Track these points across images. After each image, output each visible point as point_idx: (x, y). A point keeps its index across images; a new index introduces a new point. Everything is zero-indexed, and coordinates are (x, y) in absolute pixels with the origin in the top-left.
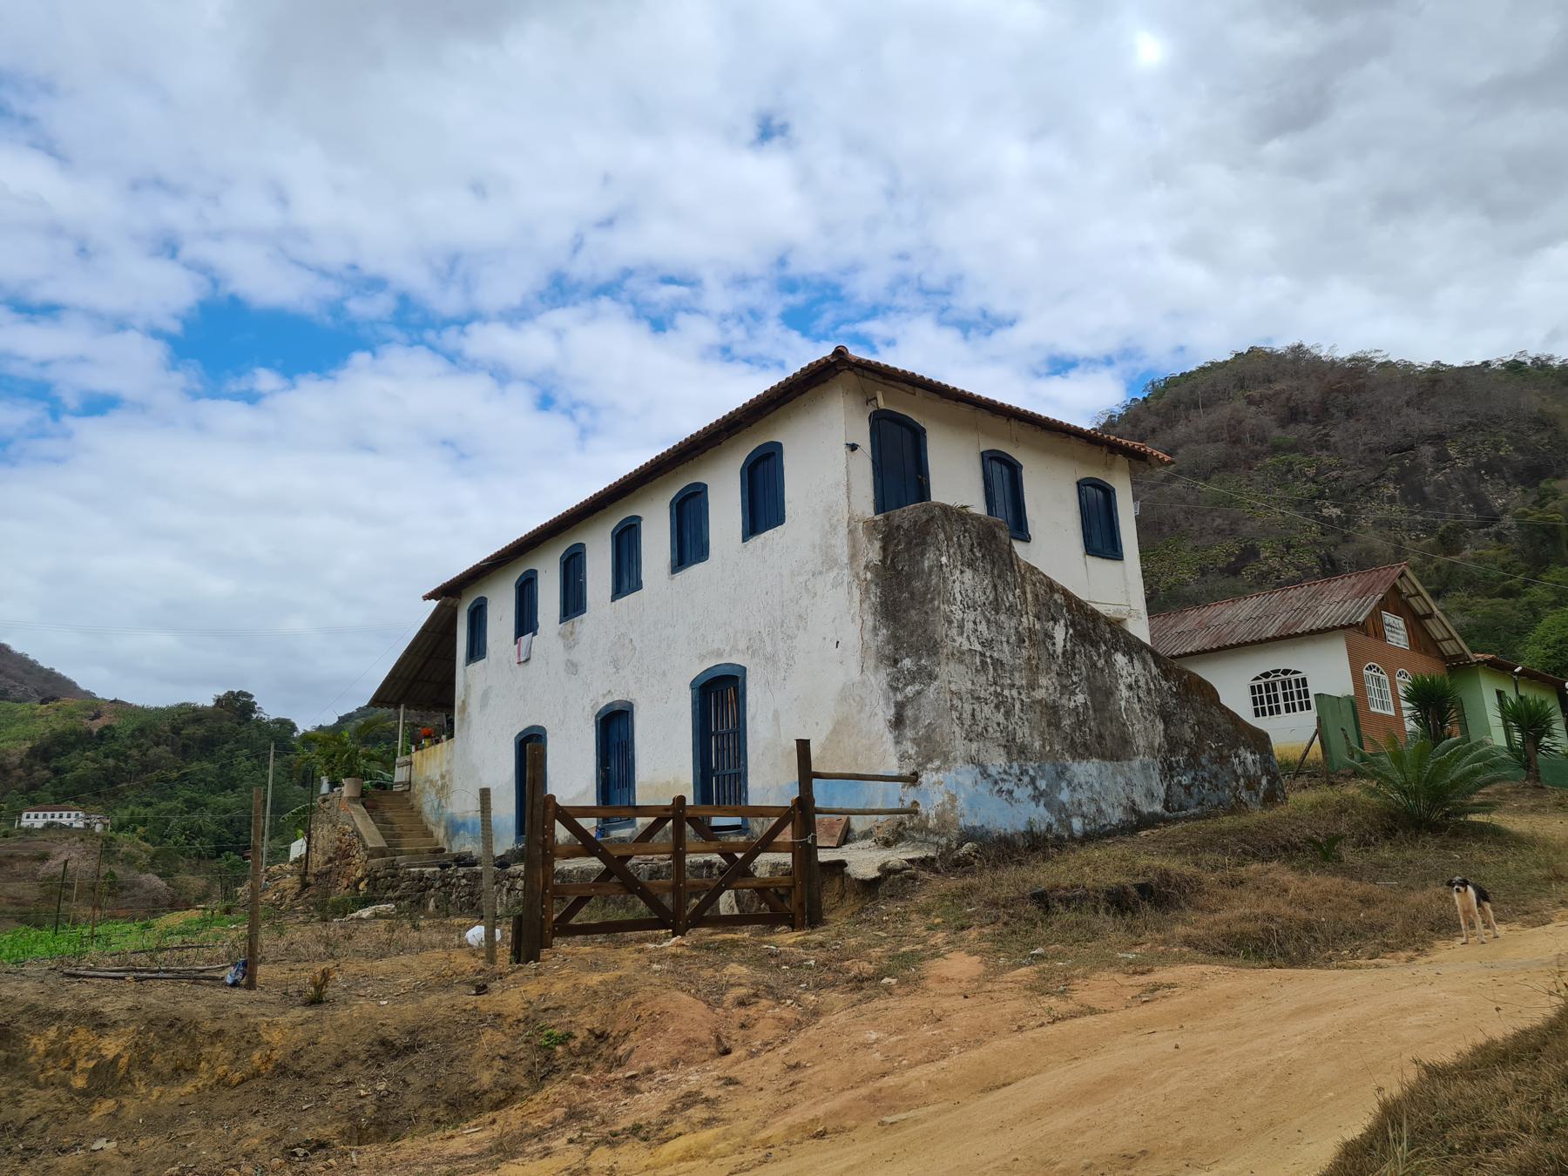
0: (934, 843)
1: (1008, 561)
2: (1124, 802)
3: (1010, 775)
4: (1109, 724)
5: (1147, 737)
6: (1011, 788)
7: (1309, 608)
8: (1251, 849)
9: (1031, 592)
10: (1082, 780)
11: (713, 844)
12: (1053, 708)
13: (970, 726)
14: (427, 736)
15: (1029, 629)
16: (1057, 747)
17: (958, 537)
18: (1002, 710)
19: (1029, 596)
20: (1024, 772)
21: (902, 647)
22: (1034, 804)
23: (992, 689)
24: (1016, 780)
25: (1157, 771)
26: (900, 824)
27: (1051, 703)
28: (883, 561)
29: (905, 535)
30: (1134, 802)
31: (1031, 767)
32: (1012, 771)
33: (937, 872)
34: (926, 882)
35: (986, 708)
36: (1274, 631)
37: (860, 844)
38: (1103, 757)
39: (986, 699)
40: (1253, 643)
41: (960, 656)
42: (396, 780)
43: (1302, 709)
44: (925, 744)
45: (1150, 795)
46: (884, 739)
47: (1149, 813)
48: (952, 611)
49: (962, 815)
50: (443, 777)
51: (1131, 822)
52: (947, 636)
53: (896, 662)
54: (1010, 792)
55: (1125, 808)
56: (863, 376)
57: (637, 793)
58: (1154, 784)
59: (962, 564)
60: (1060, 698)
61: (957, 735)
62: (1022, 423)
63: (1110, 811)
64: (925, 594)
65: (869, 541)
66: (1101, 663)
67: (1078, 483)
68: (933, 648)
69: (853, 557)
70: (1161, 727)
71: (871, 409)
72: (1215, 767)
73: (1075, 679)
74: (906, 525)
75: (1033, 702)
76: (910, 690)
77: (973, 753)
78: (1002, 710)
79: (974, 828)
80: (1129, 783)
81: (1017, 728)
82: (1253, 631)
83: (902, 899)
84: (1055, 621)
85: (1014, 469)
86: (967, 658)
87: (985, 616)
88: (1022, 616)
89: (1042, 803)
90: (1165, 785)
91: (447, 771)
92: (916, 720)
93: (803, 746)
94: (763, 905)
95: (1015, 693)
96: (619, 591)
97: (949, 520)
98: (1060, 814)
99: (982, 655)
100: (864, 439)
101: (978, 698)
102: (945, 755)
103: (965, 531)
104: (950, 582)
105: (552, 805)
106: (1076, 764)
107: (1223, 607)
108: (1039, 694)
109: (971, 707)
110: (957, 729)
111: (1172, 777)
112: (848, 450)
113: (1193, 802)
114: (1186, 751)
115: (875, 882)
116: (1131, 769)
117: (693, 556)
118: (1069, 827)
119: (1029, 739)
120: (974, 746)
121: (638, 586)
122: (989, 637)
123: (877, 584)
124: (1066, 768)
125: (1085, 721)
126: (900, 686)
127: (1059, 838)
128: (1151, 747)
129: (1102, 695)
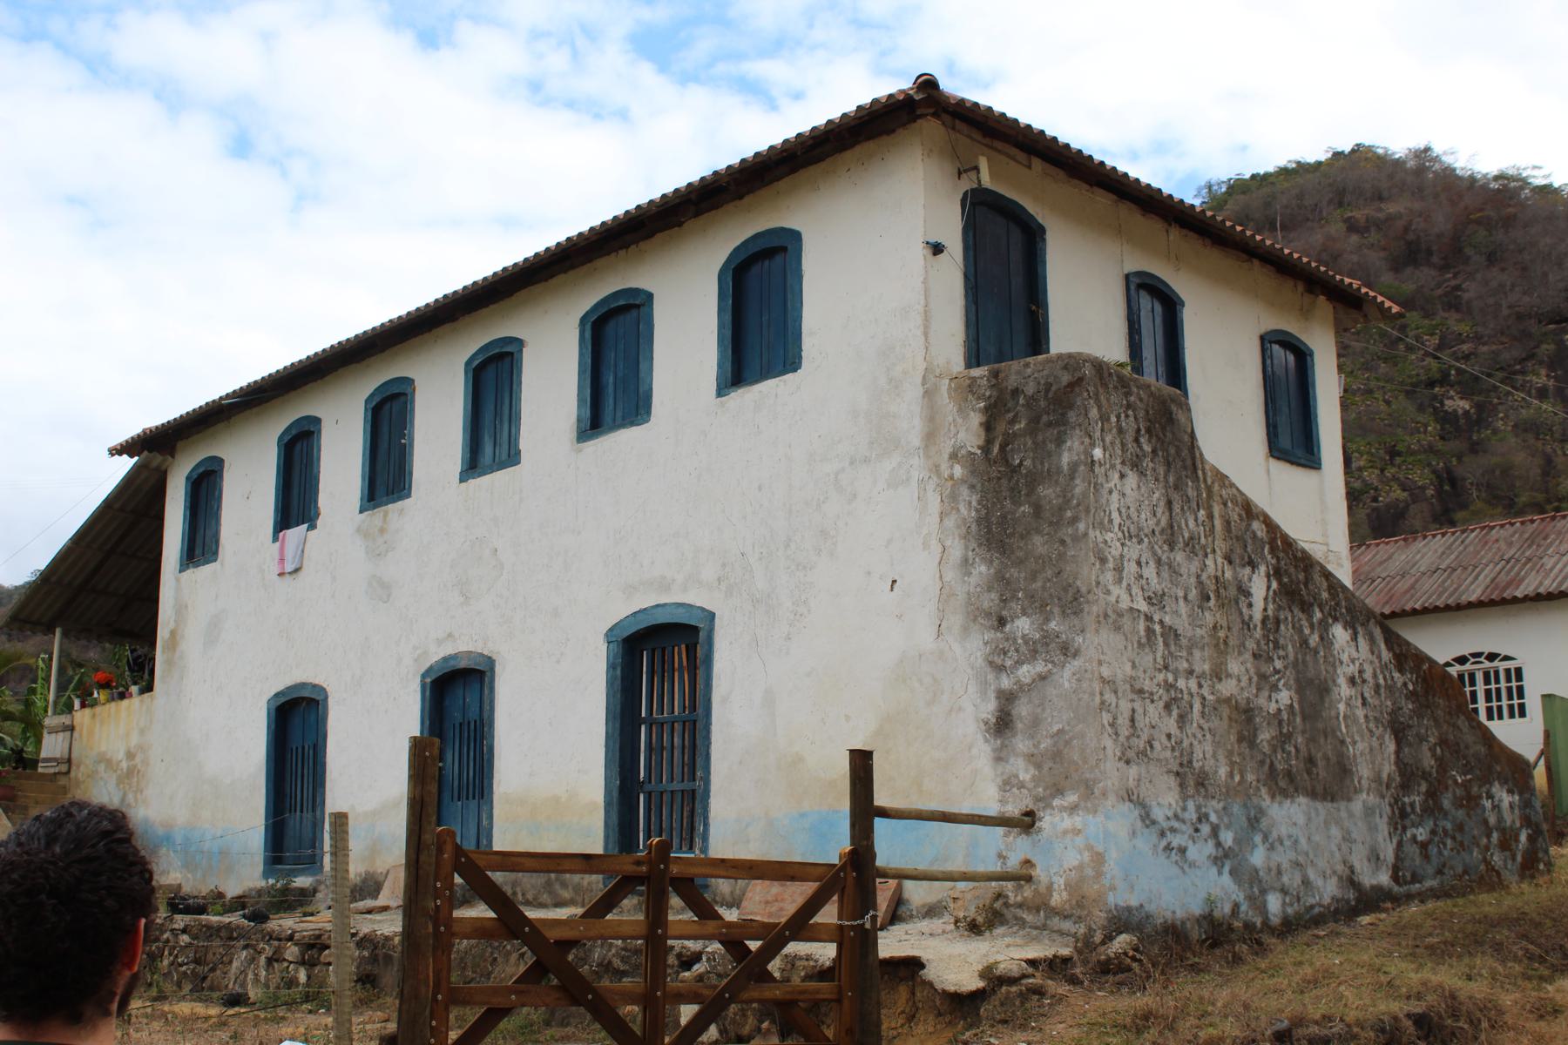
0: (1061, 933)
1: (1189, 462)
2: (1340, 868)
3: (1183, 821)
4: (1322, 741)
5: (1373, 763)
6: (1184, 844)
7: (1529, 560)
8: (1537, 951)
9: (1222, 516)
10: (1284, 831)
11: (711, 926)
13: (1128, 738)
14: (105, 685)
15: (1217, 578)
16: (1250, 777)
17: (1118, 417)
18: (1175, 713)
19: (1218, 522)
20: (1203, 818)
21: (1014, 597)
22: (1214, 870)
23: (1161, 677)
24: (1191, 831)
25: (1385, 819)
26: (999, 896)
27: (1243, 703)
28: (986, 448)
29: (1028, 405)
31: (1213, 808)
32: (1187, 816)
33: (1074, 981)
34: (1060, 999)
35: (1151, 708)
36: (1479, 591)
37: (924, 925)
38: (1313, 795)
40: (1448, 608)
41: (1114, 619)
42: (43, 755)
43: (1512, 716)
44: (1051, 764)
45: (1375, 858)
46: (975, 751)
47: (1373, 887)
48: (1106, 541)
49: (1113, 888)
50: (130, 755)
51: (1348, 901)
52: (1098, 583)
53: (1002, 622)
54: (1183, 851)
55: (1340, 878)
56: (953, 128)
57: (496, 812)
58: (1380, 839)
59: (1123, 463)
61: (1109, 752)
62: (1185, 231)
63: (1320, 882)
64: (1061, 509)
65: (960, 410)
66: (1314, 640)
67: (1262, 338)
68: (1073, 603)
69: (930, 437)
70: (1391, 747)
71: (967, 184)
72: (1461, 814)
73: (1278, 664)
74: (1030, 389)
75: (1219, 701)
76: (1026, 672)
77: (1131, 783)
78: (1175, 713)
79: (1129, 909)
80: (1347, 838)
81: (1195, 743)
82: (1446, 590)
83: (1023, 1027)
84: (1253, 565)
85: (1170, 306)
86: (1126, 622)
87: (1154, 554)
88: (1206, 555)
89: (1227, 869)
90: (1395, 841)
91: (141, 747)
92: (1036, 722)
93: (861, 763)
94: (765, 1025)
96: (474, 465)
97: (1105, 386)
98: (1252, 887)
99: (1149, 618)
100: (952, 234)
101: (1141, 691)
102: (1087, 787)
103: (1129, 406)
104: (1105, 492)
105: (449, 848)
106: (1276, 805)
107: (1391, 548)
108: (1228, 688)
109: (1130, 705)
110: (1109, 743)
111: (1404, 829)
112: (928, 252)
113: (1430, 870)
114: (1424, 787)
115: (977, 997)
116: (1351, 815)
117: (619, 414)
118: (1262, 909)
119: (1212, 762)
120: (1133, 771)
121: (512, 457)
122: (1159, 589)
123: (972, 487)
124: (1261, 812)
125: (1289, 736)
126: (1008, 663)
127: (1248, 926)
128: (1377, 779)
129: (1314, 691)
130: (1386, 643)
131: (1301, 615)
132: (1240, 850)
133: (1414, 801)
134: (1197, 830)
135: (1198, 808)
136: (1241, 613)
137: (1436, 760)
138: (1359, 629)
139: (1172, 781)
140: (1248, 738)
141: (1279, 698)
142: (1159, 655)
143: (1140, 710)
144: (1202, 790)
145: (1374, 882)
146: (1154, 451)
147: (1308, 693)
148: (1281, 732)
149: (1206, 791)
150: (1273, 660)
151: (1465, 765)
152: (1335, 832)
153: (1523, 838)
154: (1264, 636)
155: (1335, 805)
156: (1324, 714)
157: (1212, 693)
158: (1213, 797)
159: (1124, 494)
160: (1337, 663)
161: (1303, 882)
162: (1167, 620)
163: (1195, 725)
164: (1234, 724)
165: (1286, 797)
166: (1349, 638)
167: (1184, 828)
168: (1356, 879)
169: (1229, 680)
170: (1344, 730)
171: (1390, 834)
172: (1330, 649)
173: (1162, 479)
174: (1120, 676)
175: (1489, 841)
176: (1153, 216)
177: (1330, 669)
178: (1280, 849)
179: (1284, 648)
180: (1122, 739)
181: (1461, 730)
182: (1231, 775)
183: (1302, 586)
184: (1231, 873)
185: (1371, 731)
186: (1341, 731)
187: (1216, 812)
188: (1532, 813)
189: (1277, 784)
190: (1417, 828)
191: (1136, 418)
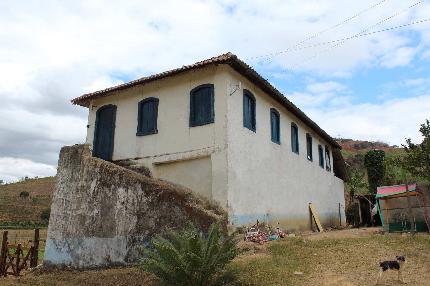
1: (79, 161)
4: (106, 221)
6: (61, 248)
10: (88, 246)
12: (84, 217)
13: (54, 226)
16: (81, 232)
17: (65, 158)
18: (65, 219)
19: (85, 173)
20: (67, 242)
22: (67, 254)
23: (63, 212)
24: (64, 245)
25: (126, 242)
30: (109, 257)
32: (63, 242)
38: (99, 236)
39: (61, 216)
45: (118, 254)
47: (116, 262)
51: (105, 265)
54: (61, 249)
55: (104, 259)
58: (122, 248)
59: (64, 167)
60: (88, 212)
66: (109, 194)
67: (190, 92)
70: (135, 220)
73: (95, 203)
75: (77, 215)
77: (53, 235)
78: (65, 219)
79: (47, 261)
80: (109, 248)
81: (68, 225)
84: (92, 180)
86: (58, 202)
87: (67, 185)
88: (80, 181)
89: (70, 254)
90: (128, 249)
95: (71, 212)
101: (59, 215)
103: (68, 154)
106: (87, 239)
108: (80, 212)
111: (133, 246)
114: (147, 232)
116: (112, 241)
118: (78, 264)
120: (54, 232)
124: (83, 241)
125: (95, 221)
127: (73, 268)
128: (126, 231)
130: (142, 189)
131: (106, 189)
132: (75, 250)
133: (141, 237)
134: (65, 245)
135: (66, 240)
136: (87, 193)
137: (156, 223)
138: (130, 187)
139: (61, 234)
140: (83, 223)
141: (94, 212)
142: (64, 207)
143: (58, 220)
144: (68, 236)
145: (117, 260)
146: (71, 162)
147: (105, 209)
148: (92, 221)
149: (69, 236)
150: (94, 202)
151: (173, 224)
152: (105, 246)
154: (93, 197)
155: (106, 239)
156: (109, 214)
157: (75, 213)
158: (70, 237)
159: (63, 174)
160: (117, 199)
161: (90, 259)
162: (67, 199)
163: (69, 221)
164: (80, 220)
165: (90, 237)
167: (62, 244)
168: (110, 259)
169: (81, 210)
170: (116, 218)
171: (126, 247)
172: (115, 196)
173: (72, 167)
174: (55, 213)
176: (152, 81)
178: (86, 250)
180: (53, 226)
181: (175, 212)
182: (76, 232)
183: (109, 181)
184: (71, 255)
186: (115, 218)
187: (70, 241)
189: (88, 234)
190: (140, 245)
191: (69, 156)
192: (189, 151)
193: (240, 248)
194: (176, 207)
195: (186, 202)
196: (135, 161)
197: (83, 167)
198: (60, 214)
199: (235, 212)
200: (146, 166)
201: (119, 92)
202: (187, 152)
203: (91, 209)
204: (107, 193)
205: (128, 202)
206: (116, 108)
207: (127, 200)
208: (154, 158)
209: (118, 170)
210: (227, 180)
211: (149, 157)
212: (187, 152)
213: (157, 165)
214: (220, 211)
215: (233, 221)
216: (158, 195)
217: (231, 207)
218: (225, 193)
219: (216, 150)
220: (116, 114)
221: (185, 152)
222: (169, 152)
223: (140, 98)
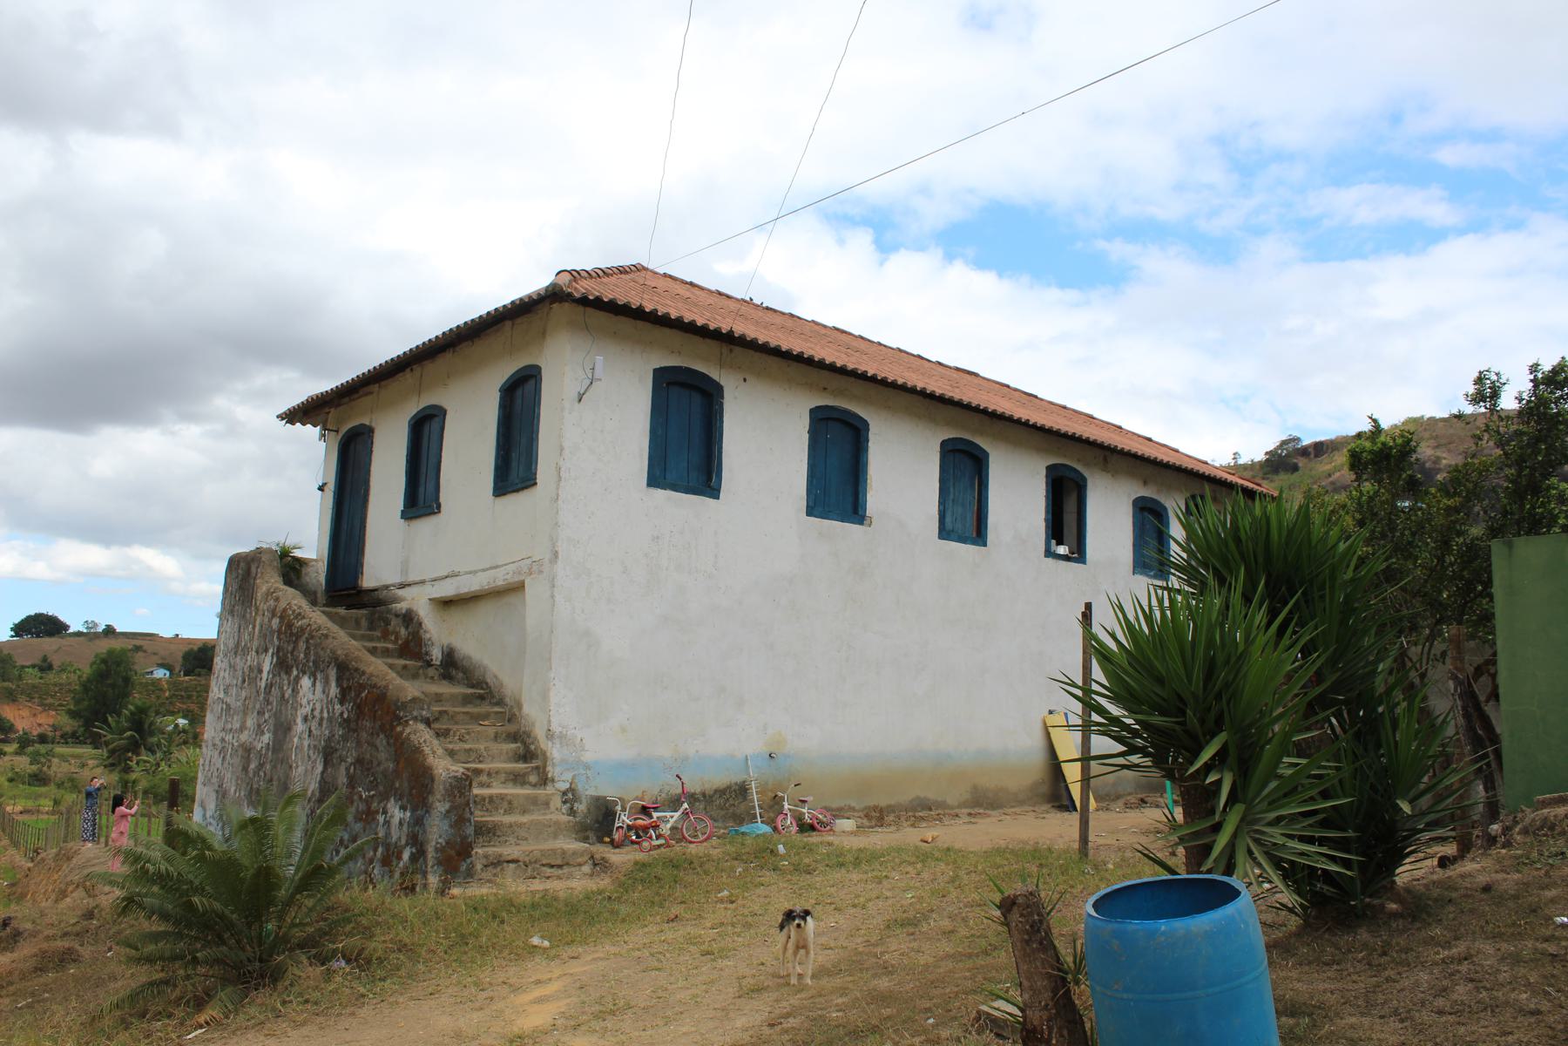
70: (320, 768)
72: (358, 827)
75: (239, 746)
84: (266, 651)
108: (244, 737)
129: (283, 729)
130: (339, 680)
136: (256, 686)
150: (264, 713)
151: (371, 782)
153: (406, 855)
166: (310, 685)
170: (293, 758)
175: (375, 854)
177: (294, 712)
179: (271, 704)
181: (377, 749)
183: (289, 655)
185: (309, 757)
188: (421, 832)
192: (491, 568)
193: (521, 859)
194: (382, 736)
195: (400, 724)
196: (400, 592)
197: (256, 614)
198: (217, 742)
199: (583, 750)
200: (415, 609)
201: (379, 387)
202: (487, 569)
203: (260, 731)
204: (285, 688)
205: (314, 717)
206: (373, 437)
207: (312, 710)
208: (433, 586)
209: (309, 625)
210: (550, 659)
211: (423, 582)
212: (487, 569)
213: (446, 604)
214: (532, 747)
215: (572, 780)
216: (358, 701)
217: (562, 737)
218: (545, 696)
219: (535, 568)
220: (372, 451)
221: (484, 570)
222: (457, 570)
223: (412, 408)
